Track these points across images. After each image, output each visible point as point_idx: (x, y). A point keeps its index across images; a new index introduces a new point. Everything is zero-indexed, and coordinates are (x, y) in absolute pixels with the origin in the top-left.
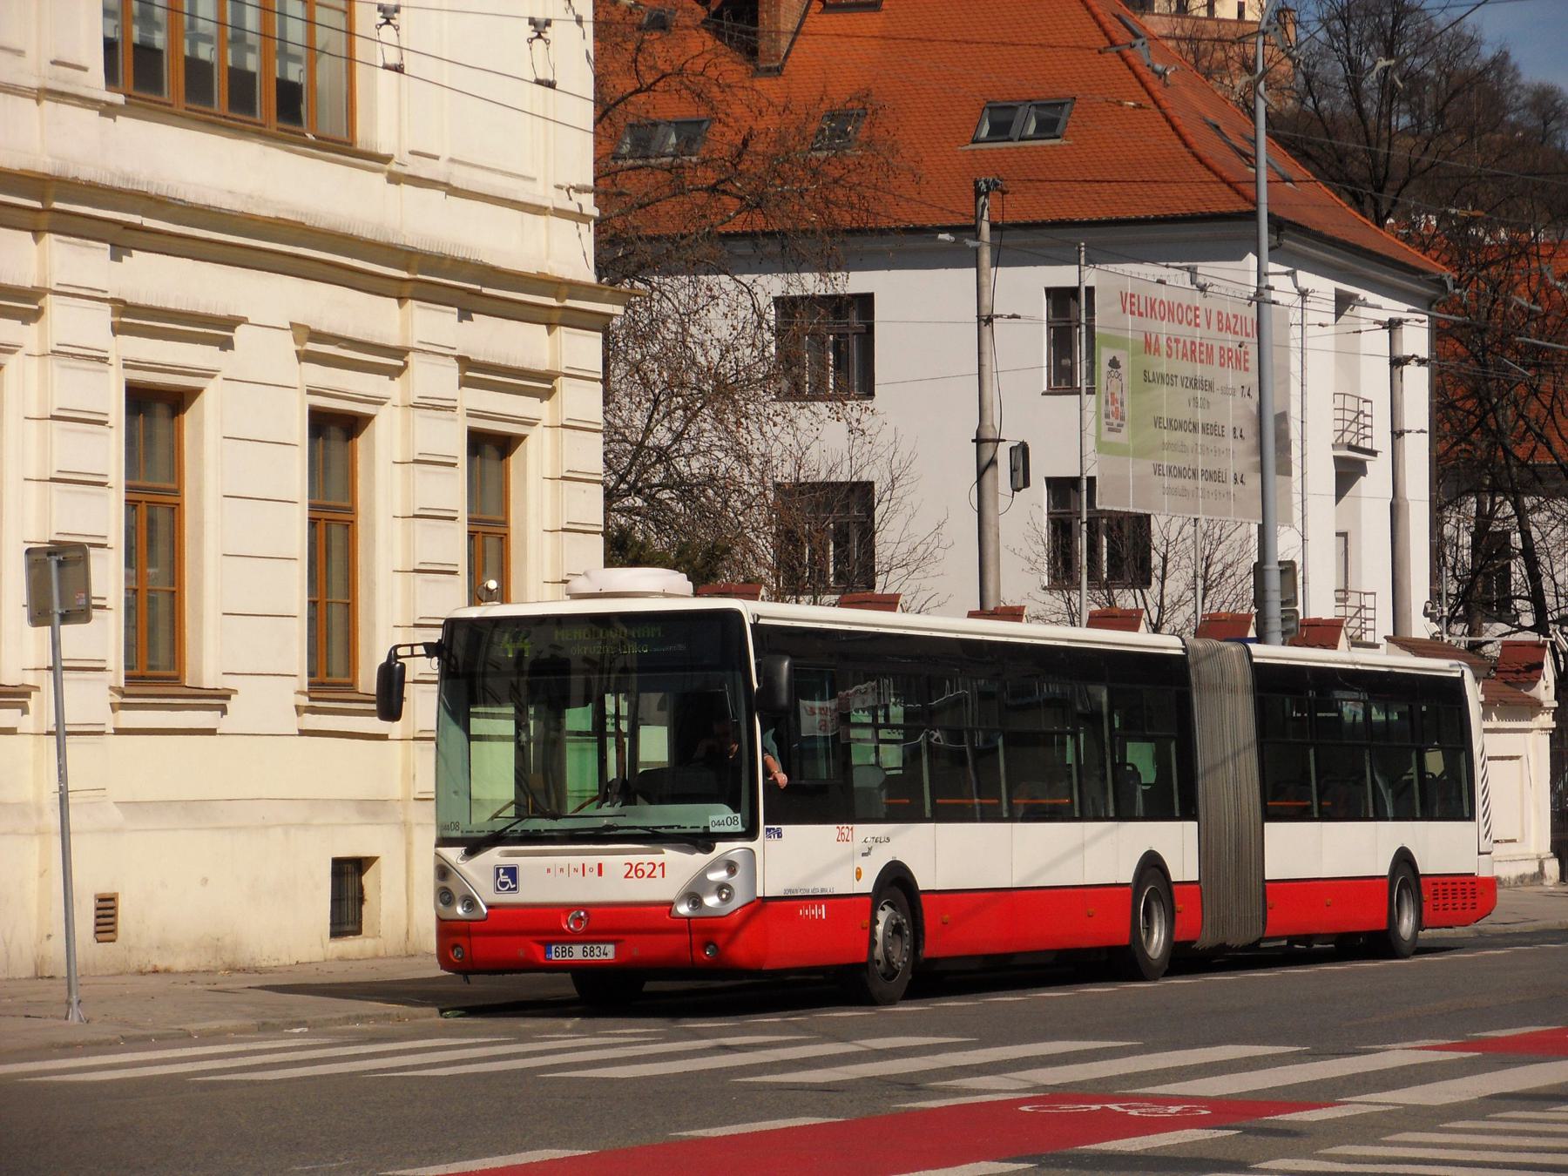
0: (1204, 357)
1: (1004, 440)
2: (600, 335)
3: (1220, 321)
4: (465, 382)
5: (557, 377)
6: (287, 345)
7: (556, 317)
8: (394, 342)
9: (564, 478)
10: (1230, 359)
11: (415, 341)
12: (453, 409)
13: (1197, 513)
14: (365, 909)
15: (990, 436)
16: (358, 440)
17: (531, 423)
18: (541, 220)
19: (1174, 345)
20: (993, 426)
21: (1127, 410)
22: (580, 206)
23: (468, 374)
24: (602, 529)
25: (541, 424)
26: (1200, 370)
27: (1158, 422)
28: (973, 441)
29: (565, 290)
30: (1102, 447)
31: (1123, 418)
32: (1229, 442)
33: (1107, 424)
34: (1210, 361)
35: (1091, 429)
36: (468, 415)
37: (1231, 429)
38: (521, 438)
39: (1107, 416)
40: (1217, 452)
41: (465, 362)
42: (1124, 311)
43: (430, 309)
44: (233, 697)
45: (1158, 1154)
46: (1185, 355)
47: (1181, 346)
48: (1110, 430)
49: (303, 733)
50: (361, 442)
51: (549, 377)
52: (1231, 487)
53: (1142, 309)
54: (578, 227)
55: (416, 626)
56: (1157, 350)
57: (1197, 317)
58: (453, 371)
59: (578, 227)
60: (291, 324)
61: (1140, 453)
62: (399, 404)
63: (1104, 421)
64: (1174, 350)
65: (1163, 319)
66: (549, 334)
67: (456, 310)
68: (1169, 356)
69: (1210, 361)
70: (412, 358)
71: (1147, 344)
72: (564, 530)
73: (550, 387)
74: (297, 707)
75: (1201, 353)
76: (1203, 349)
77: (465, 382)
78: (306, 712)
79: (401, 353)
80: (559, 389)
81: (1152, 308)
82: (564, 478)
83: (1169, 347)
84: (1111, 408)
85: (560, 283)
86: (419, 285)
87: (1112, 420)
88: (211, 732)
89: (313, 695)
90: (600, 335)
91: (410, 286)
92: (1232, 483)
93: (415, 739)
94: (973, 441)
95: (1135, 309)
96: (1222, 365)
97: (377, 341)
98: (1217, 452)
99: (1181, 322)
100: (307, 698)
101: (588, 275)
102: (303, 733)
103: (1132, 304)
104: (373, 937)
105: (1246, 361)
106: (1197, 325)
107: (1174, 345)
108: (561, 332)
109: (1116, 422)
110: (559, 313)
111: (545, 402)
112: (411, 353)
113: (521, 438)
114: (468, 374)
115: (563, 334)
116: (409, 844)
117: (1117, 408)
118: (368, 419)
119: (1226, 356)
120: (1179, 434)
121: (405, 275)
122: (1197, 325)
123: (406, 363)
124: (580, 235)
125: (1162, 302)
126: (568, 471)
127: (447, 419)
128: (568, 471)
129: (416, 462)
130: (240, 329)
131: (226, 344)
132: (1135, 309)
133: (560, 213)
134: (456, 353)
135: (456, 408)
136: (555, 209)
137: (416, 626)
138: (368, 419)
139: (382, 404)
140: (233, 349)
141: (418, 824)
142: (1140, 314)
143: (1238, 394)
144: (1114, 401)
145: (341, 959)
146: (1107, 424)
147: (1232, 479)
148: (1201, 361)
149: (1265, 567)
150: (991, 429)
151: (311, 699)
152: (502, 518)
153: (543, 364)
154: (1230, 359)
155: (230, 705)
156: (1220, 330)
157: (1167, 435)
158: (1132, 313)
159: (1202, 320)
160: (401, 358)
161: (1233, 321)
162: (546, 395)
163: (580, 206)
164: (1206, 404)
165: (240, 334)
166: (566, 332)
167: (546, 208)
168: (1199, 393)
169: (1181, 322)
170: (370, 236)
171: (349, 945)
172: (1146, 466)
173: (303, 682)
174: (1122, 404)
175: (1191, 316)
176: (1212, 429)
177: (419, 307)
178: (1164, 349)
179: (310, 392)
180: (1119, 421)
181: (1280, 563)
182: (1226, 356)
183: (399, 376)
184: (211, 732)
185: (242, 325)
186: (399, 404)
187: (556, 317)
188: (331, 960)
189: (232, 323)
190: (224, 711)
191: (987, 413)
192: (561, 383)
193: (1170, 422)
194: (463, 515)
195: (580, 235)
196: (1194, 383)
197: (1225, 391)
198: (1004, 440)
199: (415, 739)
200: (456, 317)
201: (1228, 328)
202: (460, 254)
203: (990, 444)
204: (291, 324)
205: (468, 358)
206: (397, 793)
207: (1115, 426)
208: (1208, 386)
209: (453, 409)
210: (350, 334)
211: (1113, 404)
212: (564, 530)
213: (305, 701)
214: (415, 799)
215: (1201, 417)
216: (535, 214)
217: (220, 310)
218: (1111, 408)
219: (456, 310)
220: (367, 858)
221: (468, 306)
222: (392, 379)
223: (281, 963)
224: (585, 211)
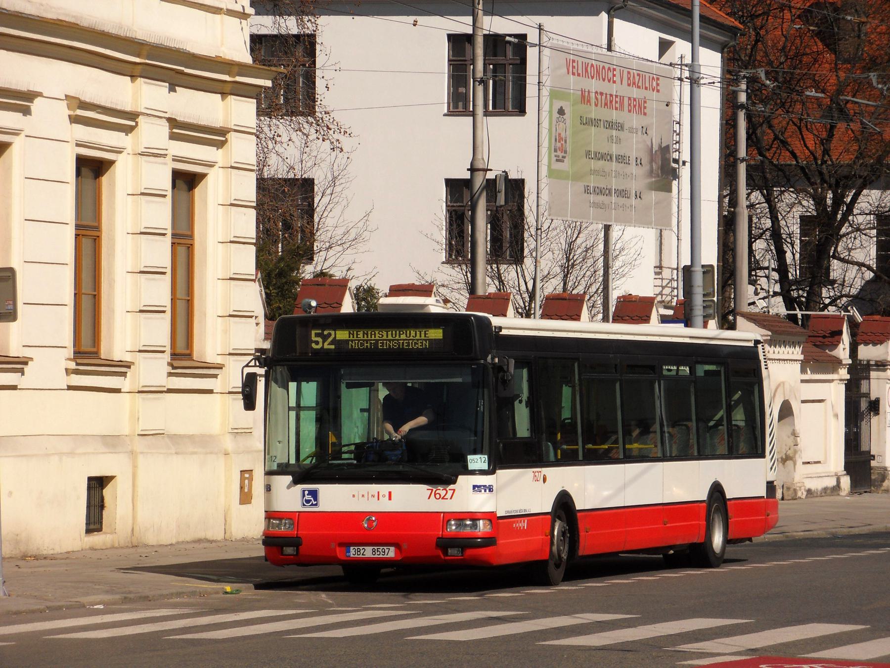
0: (618, 105)
1: (491, 170)
2: (255, 101)
3: (629, 79)
4: (173, 137)
6: (63, 111)
7: (228, 88)
8: (128, 108)
9: (232, 205)
10: (635, 106)
11: (143, 107)
13: (611, 221)
14: (105, 513)
15: (481, 166)
16: (103, 178)
17: (211, 165)
18: (218, 17)
19: (599, 97)
20: (483, 159)
22: (243, 7)
23: (175, 130)
24: (254, 241)
25: (217, 166)
26: (614, 115)
27: (588, 153)
28: (468, 170)
29: (236, 69)
30: (552, 173)
31: (566, 152)
32: (633, 169)
33: (556, 156)
34: (622, 108)
35: (545, 161)
36: (174, 160)
37: (635, 158)
38: (203, 176)
39: (555, 151)
40: (625, 176)
41: (173, 122)
42: (568, 73)
44: (30, 363)
46: (606, 104)
47: (604, 97)
48: (557, 160)
49: (70, 388)
50: (105, 179)
51: (223, 132)
52: (633, 201)
54: (241, 23)
55: (141, 311)
56: (589, 101)
57: (614, 75)
58: (164, 129)
59: (241, 23)
60: (66, 96)
62: (131, 152)
63: (553, 154)
64: (600, 100)
65: (593, 78)
67: (168, 84)
68: (596, 105)
69: (622, 108)
70: (141, 119)
71: (583, 96)
72: (231, 242)
73: (224, 139)
74: (66, 370)
75: (616, 102)
76: (618, 100)
77: (173, 137)
78: (73, 373)
79: (133, 116)
80: (229, 140)
82: (232, 205)
83: (596, 98)
84: (559, 145)
85: (232, 64)
86: (145, 67)
87: (559, 153)
88: (14, 388)
89: (79, 361)
90: (255, 101)
91: (140, 67)
92: (634, 198)
93: (139, 392)
94: (468, 170)
95: (575, 71)
96: (630, 111)
97: (119, 108)
98: (625, 176)
99: (604, 80)
100: (75, 364)
102: (70, 388)
103: (574, 67)
104: (111, 533)
105: (645, 108)
106: (614, 82)
107: (599, 97)
108: (231, 99)
109: (561, 154)
110: (230, 85)
111: (219, 150)
112: (140, 117)
113: (203, 176)
114: (175, 130)
115: (232, 100)
116: (135, 467)
117: (562, 144)
118: (111, 163)
119: (632, 105)
120: (601, 162)
121: (137, 60)
122: (614, 82)
123: (137, 123)
124: (242, 29)
125: (592, 65)
126: (235, 200)
127: (160, 163)
128: (235, 200)
129: (142, 194)
130: (38, 101)
131: (26, 111)
132: (575, 71)
133: (231, 13)
134: (167, 116)
135: (166, 155)
136: (227, 9)
137: (141, 311)
138: (111, 163)
139: (120, 152)
140: (30, 114)
141: (142, 453)
142: (579, 75)
143: (640, 133)
144: (561, 139)
145: (92, 549)
146: (556, 156)
147: (634, 195)
148: (616, 109)
149: (693, 269)
150: (482, 161)
151: (77, 364)
152: (189, 233)
154: (635, 106)
155: (27, 369)
156: (629, 85)
157: (595, 164)
158: (573, 74)
160: (133, 119)
161: (637, 78)
162: (220, 145)
163: (243, 7)
164: (619, 141)
165: (37, 105)
166: (235, 100)
167: (221, 9)
168: (614, 133)
170: (113, 31)
171: (97, 539)
172: (580, 187)
173: (70, 352)
174: (566, 142)
175: (610, 75)
176: (622, 159)
177: (145, 83)
178: (593, 100)
179: (77, 145)
180: (563, 154)
181: (703, 266)
182: (632, 105)
183: (131, 133)
184: (14, 388)
185: (39, 98)
186: (131, 152)
187: (228, 88)
188: (86, 550)
189: (31, 96)
190: (22, 372)
191: (479, 150)
192: (231, 136)
193: (595, 153)
194: (169, 232)
195: (242, 29)
196: (610, 125)
197: (631, 130)
198: (491, 170)
199: (139, 392)
200: (167, 89)
201: (634, 83)
202: (172, 45)
203: (481, 173)
204: (66, 96)
205: (175, 120)
206: (126, 431)
207: (560, 158)
208: (620, 127)
210: (103, 103)
211: (559, 142)
212: (231, 242)
213: (72, 365)
214: (138, 435)
215: (615, 150)
216: (214, 13)
217: (24, 88)
218: (559, 145)
219: (168, 84)
220: (107, 477)
221: (175, 81)
222: (127, 135)
223: (55, 552)
224: (246, 12)
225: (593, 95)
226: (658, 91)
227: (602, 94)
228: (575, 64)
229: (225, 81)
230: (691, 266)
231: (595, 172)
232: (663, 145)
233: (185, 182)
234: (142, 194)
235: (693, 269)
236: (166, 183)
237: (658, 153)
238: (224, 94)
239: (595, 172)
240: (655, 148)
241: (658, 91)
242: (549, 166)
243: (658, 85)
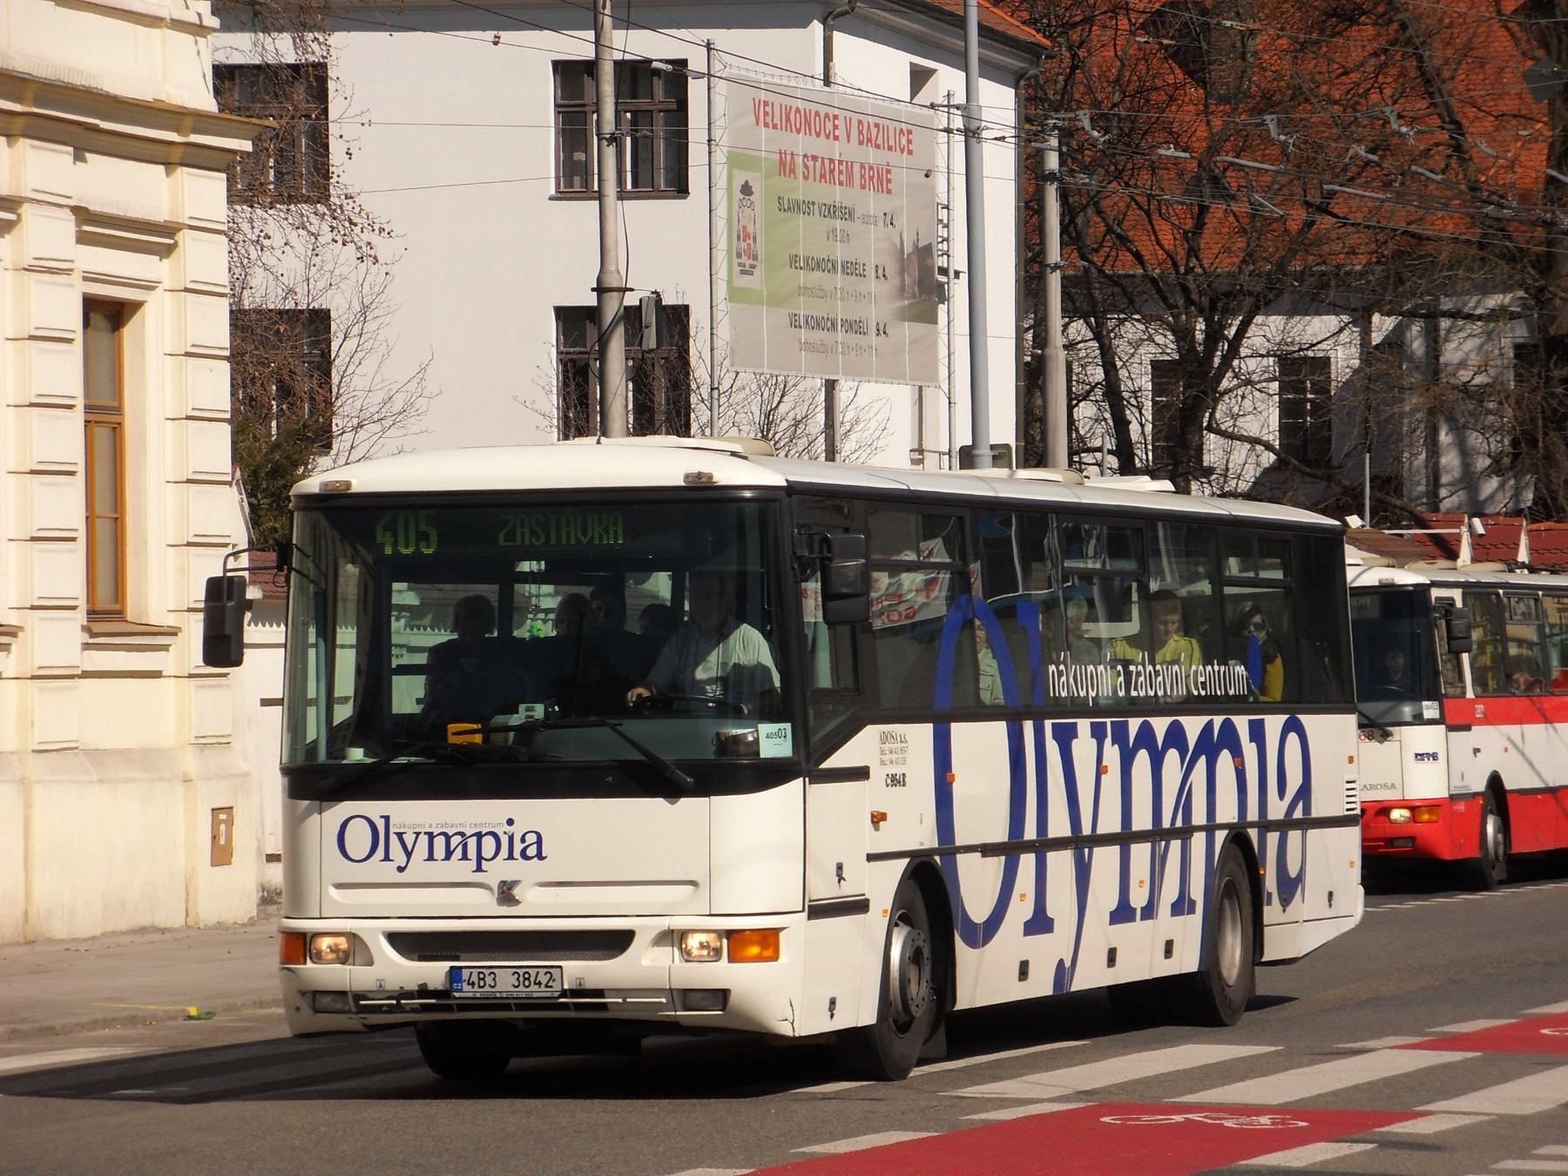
0: (843, 178)
2: (224, 176)
3: (860, 132)
4: (83, 238)
5: (180, 230)
7: (177, 155)
9: (188, 354)
10: (871, 178)
12: (68, 272)
15: (615, 284)
18: (155, 33)
19: (810, 163)
21: (761, 249)
22: (199, 15)
23: (86, 228)
24: (228, 416)
25: (161, 287)
26: (837, 194)
27: (794, 259)
28: (593, 290)
29: (189, 122)
30: (734, 294)
31: (755, 258)
32: (872, 285)
33: (740, 265)
34: (850, 183)
35: (722, 273)
36: (85, 279)
37: (873, 267)
39: (739, 256)
40: (859, 296)
42: (757, 124)
43: (45, 149)
45: (1331, 1168)
46: (823, 176)
47: (818, 164)
48: (743, 272)
51: (169, 229)
52: (873, 339)
53: (777, 121)
54: (196, 42)
55: (33, 539)
56: (793, 171)
57: (836, 127)
58: (67, 225)
59: (196, 42)
61: (775, 301)
62: (10, 267)
63: (736, 261)
65: (798, 131)
66: (167, 176)
67: (71, 149)
68: (806, 178)
69: (850, 183)
70: (26, 209)
71: (782, 163)
73: (172, 242)
75: (840, 172)
76: (843, 168)
80: (181, 243)
81: (788, 119)
82: (188, 354)
83: (806, 166)
84: (743, 245)
85: (183, 114)
87: (744, 260)
90: (224, 176)
91: (21, 121)
92: (874, 335)
93: (34, 678)
94: (593, 290)
95: (769, 119)
96: (863, 187)
98: (859, 296)
99: (818, 135)
101: (209, 104)
103: (766, 114)
105: (889, 181)
106: (836, 138)
107: (810, 163)
110: (181, 150)
114: (86, 228)
115: (185, 176)
116: (28, 806)
117: (749, 245)
119: (867, 176)
120: (817, 274)
121: (17, 107)
122: (836, 138)
123: (19, 216)
124: (199, 53)
125: (798, 110)
126: (193, 345)
127: (61, 285)
128: (193, 345)
129: (32, 338)
132: (769, 119)
133: (178, 25)
134: (71, 203)
135: (71, 270)
136: (172, 20)
137: (33, 539)
141: (39, 782)
142: (775, 127)
143: (881, 224)
144: (747, 236)
147: (874, 329)
148: (841, 183)
149: (976, 452)
150: (616, 275)
152: (115, 404)
153: (160, 212)
154: (871, 178)
156: (861, 143)
158: (766, 125)
159: (841, 132)
161: (874, 131)
162: (166, 251)
163: (199, 15)
164: (846, 238)
166: (188, 174)
167: (162, 19)
168: (838, 224)
169: (818, 135)
172: (782, 315)
174: (755, 241)
175: (829, 126)
176: (852, 268)
177: (33, 147)
178: (800, 169)
180: (751, 262)
181: (993, 447)
182: (867, 176)
186: (10, 267)
187: (177, 155)
192: (184, 237)
193: (807, 259)
194: (80, 403)
195: (199, 53)
196: (831, 211)
197: (867, 219)
199: (34, 678)
200: (71, 158)
201: (869, 140)
202: (78, 81)
203: (615, 294)
205: (86, 209)
206: (11, 744)
207: (747, 268)
208: (848, 214)
209: (68, 272)
211: (744, 241)
212: (189, 418)
214: (33, 751)
215: (840, 253)
221: (84, 142)
224: (205, 23)
225: (799, 160)
226: (910, 152)
227: (815, 158)
228: (769, 109)
229: (172, 143)
230: (973, 446)
231: (806, 291)
232: (920, 245)
233: (106, 317)
234: (32, 338)
235: (976, 452)
236: (72, 318)
237: (914, 258)
238: (169, 165)
239: (806, 291)
240: (908, 249)
241: (910, 152)
242: (730, 282)
243: (909, 142)
